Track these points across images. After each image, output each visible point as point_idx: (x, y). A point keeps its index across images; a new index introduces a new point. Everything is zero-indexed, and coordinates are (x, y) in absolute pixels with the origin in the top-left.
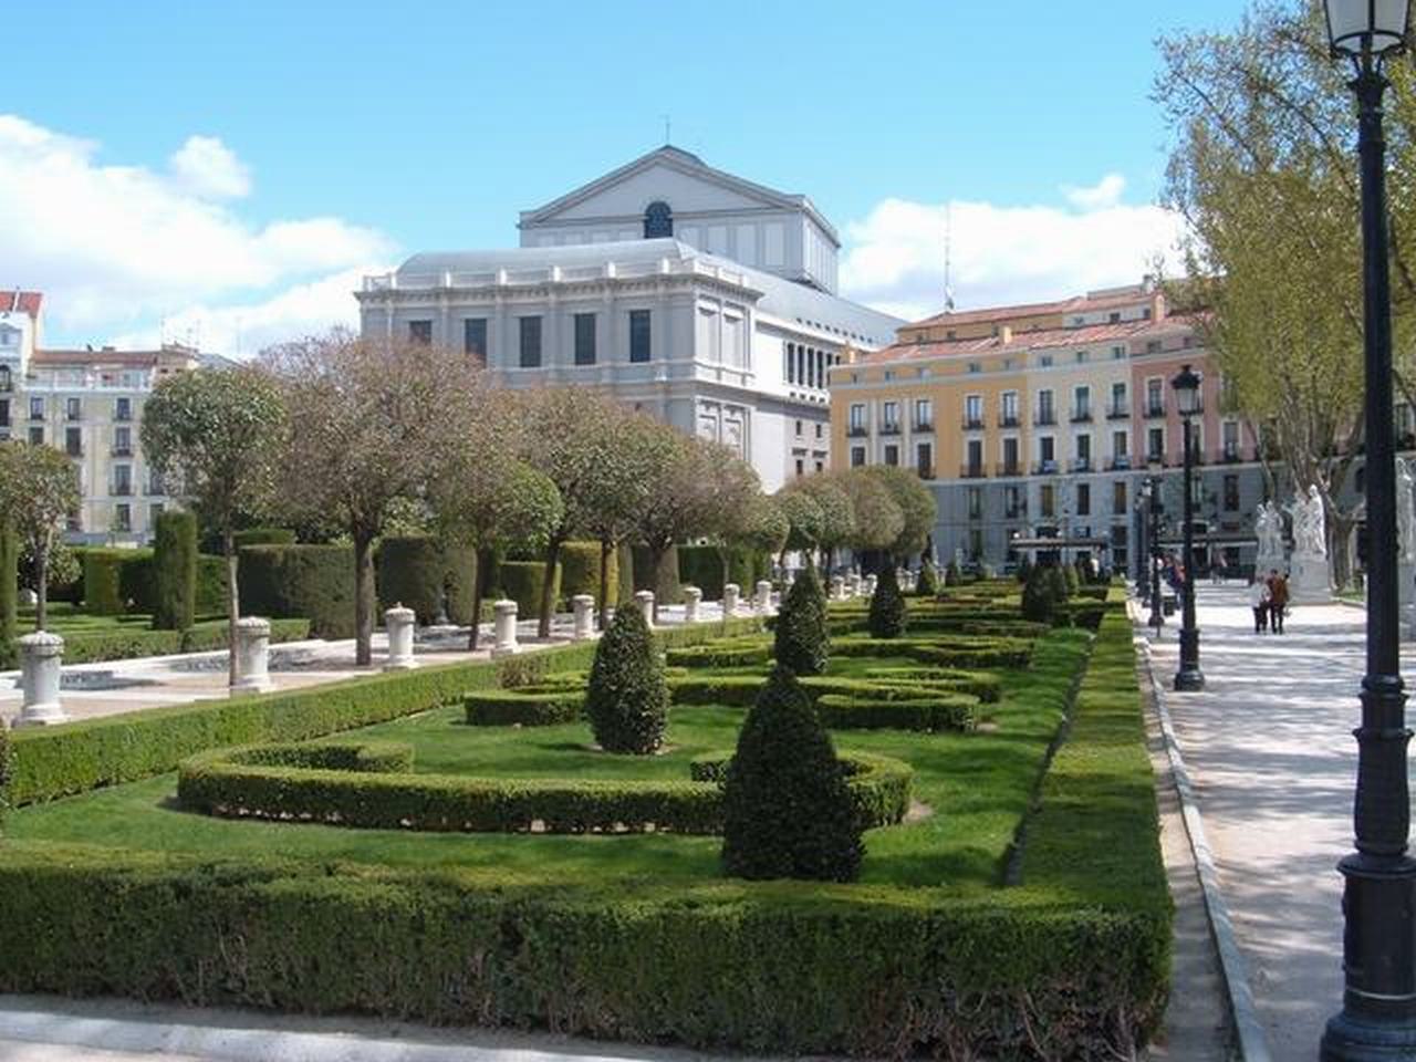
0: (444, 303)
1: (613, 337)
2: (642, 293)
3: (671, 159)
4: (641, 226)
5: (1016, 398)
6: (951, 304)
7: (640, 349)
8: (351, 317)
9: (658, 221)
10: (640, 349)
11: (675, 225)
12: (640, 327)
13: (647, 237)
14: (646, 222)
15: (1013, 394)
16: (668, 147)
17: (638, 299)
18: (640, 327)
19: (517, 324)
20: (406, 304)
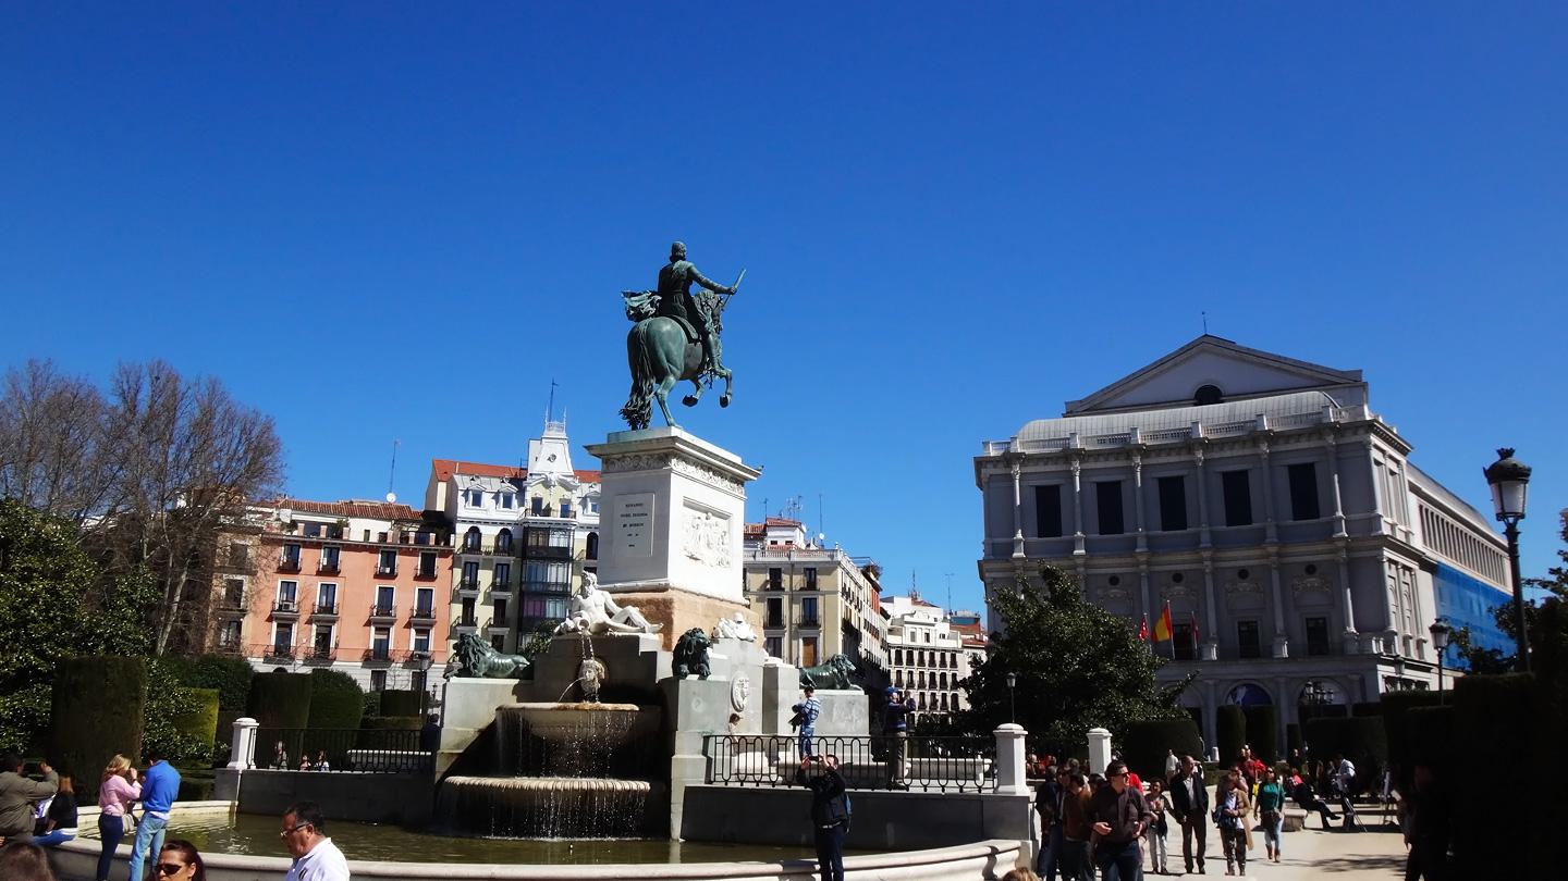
2: (1304, 445)
3: (1208, 345)
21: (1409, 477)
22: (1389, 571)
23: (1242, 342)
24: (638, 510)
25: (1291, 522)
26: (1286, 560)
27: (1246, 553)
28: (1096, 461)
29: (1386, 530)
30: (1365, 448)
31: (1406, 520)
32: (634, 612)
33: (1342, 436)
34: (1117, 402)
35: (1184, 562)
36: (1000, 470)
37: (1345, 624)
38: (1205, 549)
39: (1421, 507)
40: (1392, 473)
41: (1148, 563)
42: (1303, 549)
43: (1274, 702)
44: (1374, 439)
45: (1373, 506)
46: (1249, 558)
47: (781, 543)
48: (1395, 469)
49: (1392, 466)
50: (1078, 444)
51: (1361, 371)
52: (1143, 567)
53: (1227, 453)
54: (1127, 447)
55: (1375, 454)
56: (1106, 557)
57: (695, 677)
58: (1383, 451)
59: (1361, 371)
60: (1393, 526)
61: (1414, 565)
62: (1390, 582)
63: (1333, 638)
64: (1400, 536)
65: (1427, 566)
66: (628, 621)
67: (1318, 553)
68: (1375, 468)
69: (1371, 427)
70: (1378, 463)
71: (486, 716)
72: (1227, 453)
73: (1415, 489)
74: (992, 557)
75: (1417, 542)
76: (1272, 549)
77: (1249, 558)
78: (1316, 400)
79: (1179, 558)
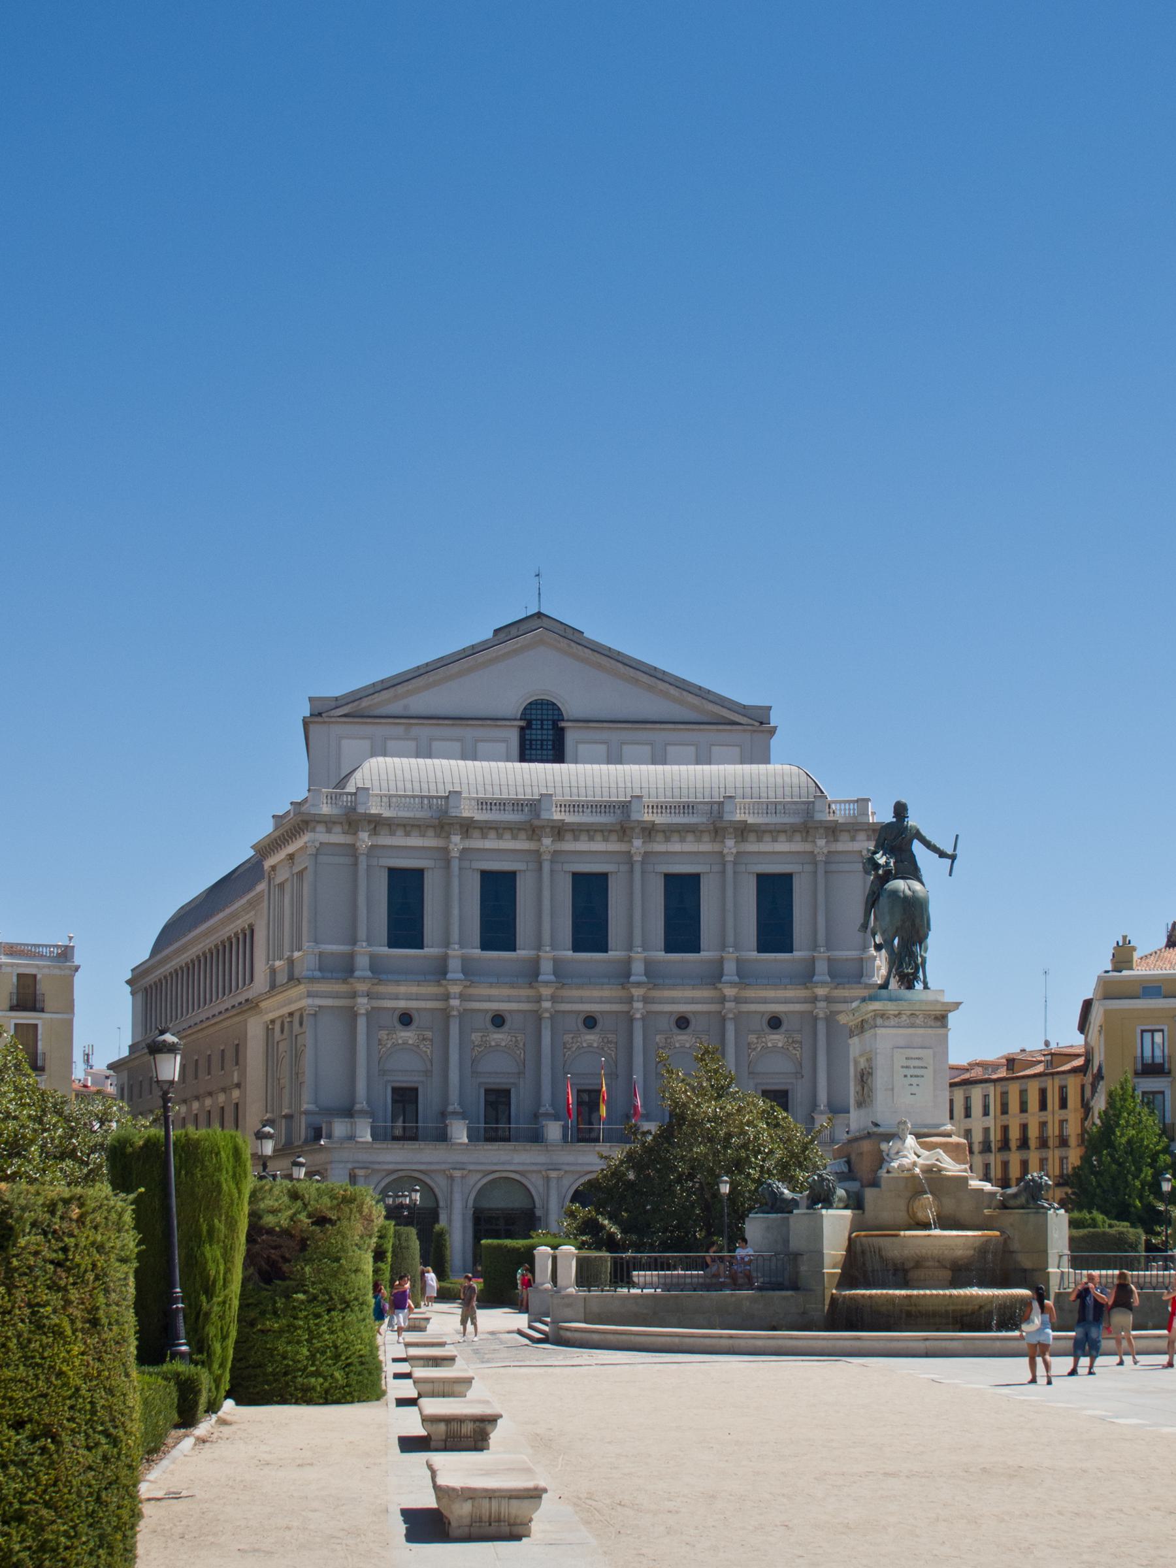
0: (457, 842)
1: (728, 913)
2: (782, 846)
4: (513, 736)
5: (1158, 1037)
7: (775, 931)
8: (252, 853)
9: (543, 734)
10: (775, 931)
11: (570, 737)
12: (775, 892)
13: (523, 758)
14: (522, 729)
15: (1153, 1031)
17: (776, 856)
18: (775, 892)
19: (569, 880)
20: (477, 843)
23: (592, 633)
24: (917, 1063)
25: (754, 954)
26: (745, 1008)
27: (689, 993)
28: (500, 837)
33: (836, 840)
34: (395, 708)
35: (602, 1001)
36: (337, 837)
38: (639, 984)
41: (554, 999)
42: (771, 994)
46: (693, 1001)
50: (467, 811)
51: (770, 708)
52: (547, 1005)
53: (676, 847)
54: (536, 822)
56: (491, 985)
59: (770, 708)
67: (786, 1001)
72: (676, 847)
74: (318, 974)
76: (730, 992)
77: (693, 1001)
78: (795, 781)
79: (596, 993)
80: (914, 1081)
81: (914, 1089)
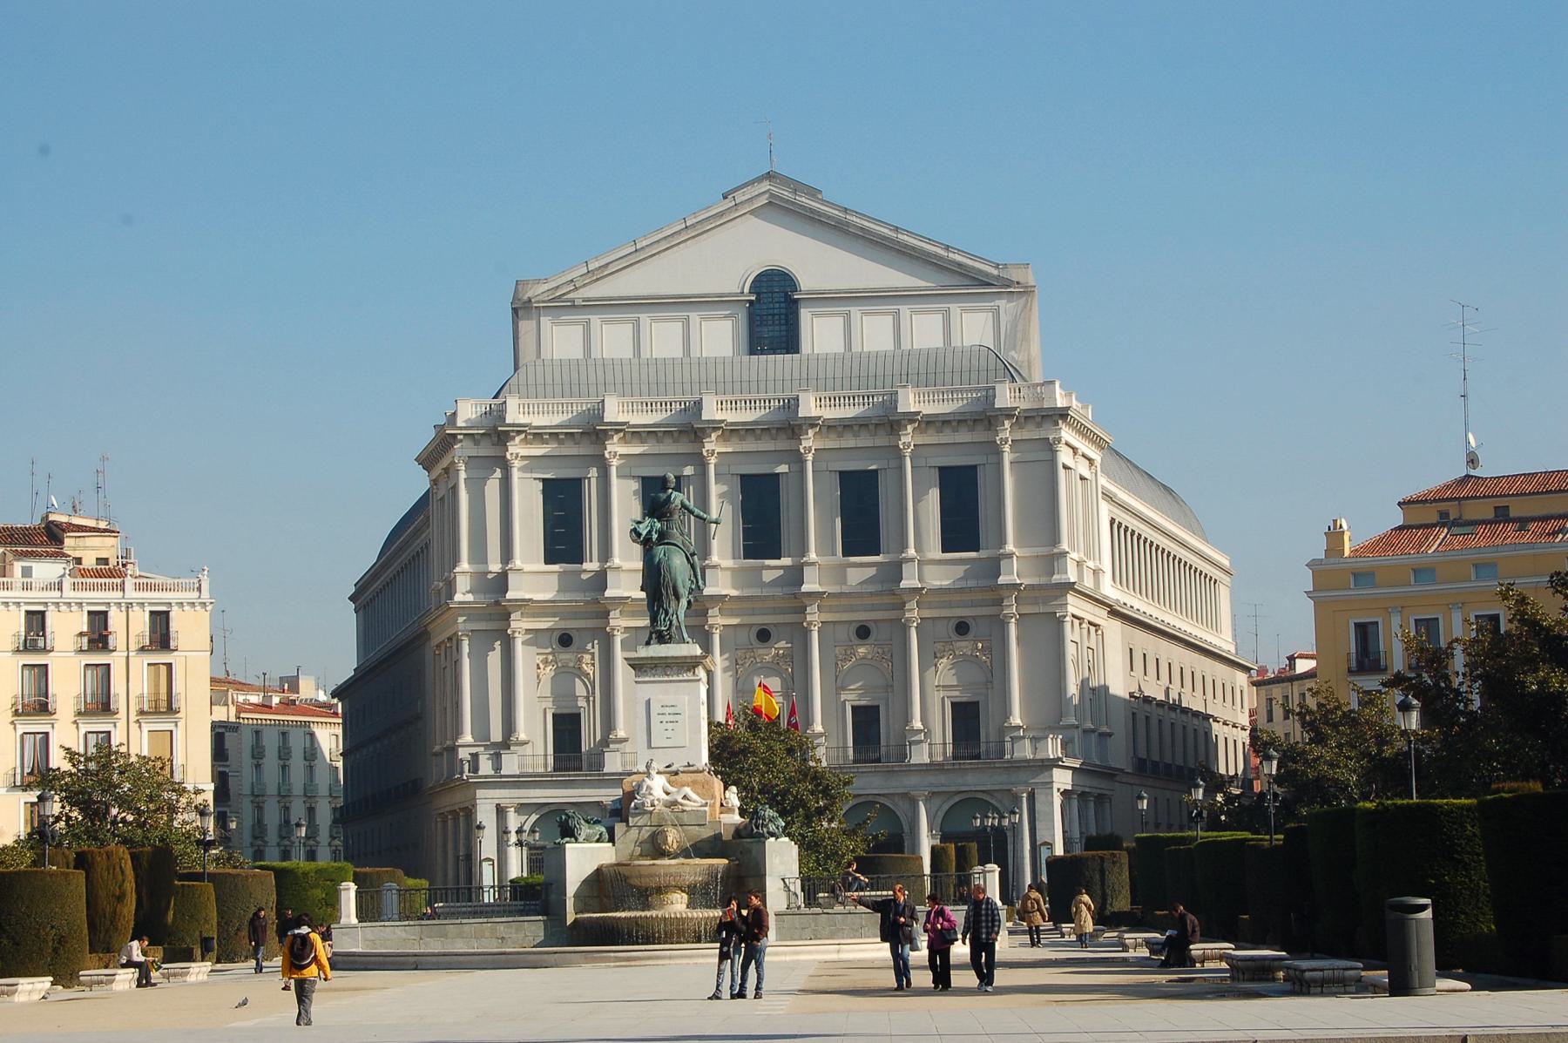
6: (1472, 461)
16: (769, 176)
21: (1103, 481)
22: (1071, 633)
29: (1072, 577)
30: (1050, 447)
31: (1092, 550)
32: (687, 790)
37: (1006, 713)
39: (1112, 521)
40: (1082, 478)
43: (906, 828)
44: (1067, 434)
45: (1055, 538)
47: (89, 562)
48: (1086, 474)
49: (1083, 468)
55: (1064, 456)
57: (772, 839)
58: (1075, 450)
60: (1079, 564)
61: (1099, 615)
62: (1070, 650)
63: (987, 731)
64: (1088, 583)
65: (1114, 613)
66: (685, 797)
68: (1062, 472)
69: (1063, 414)
70: (1066, 467)
71: (589, 870)
73: (1109, 497)
75: (1109, 590)
80: (670, 726)
81: (669, 734)
